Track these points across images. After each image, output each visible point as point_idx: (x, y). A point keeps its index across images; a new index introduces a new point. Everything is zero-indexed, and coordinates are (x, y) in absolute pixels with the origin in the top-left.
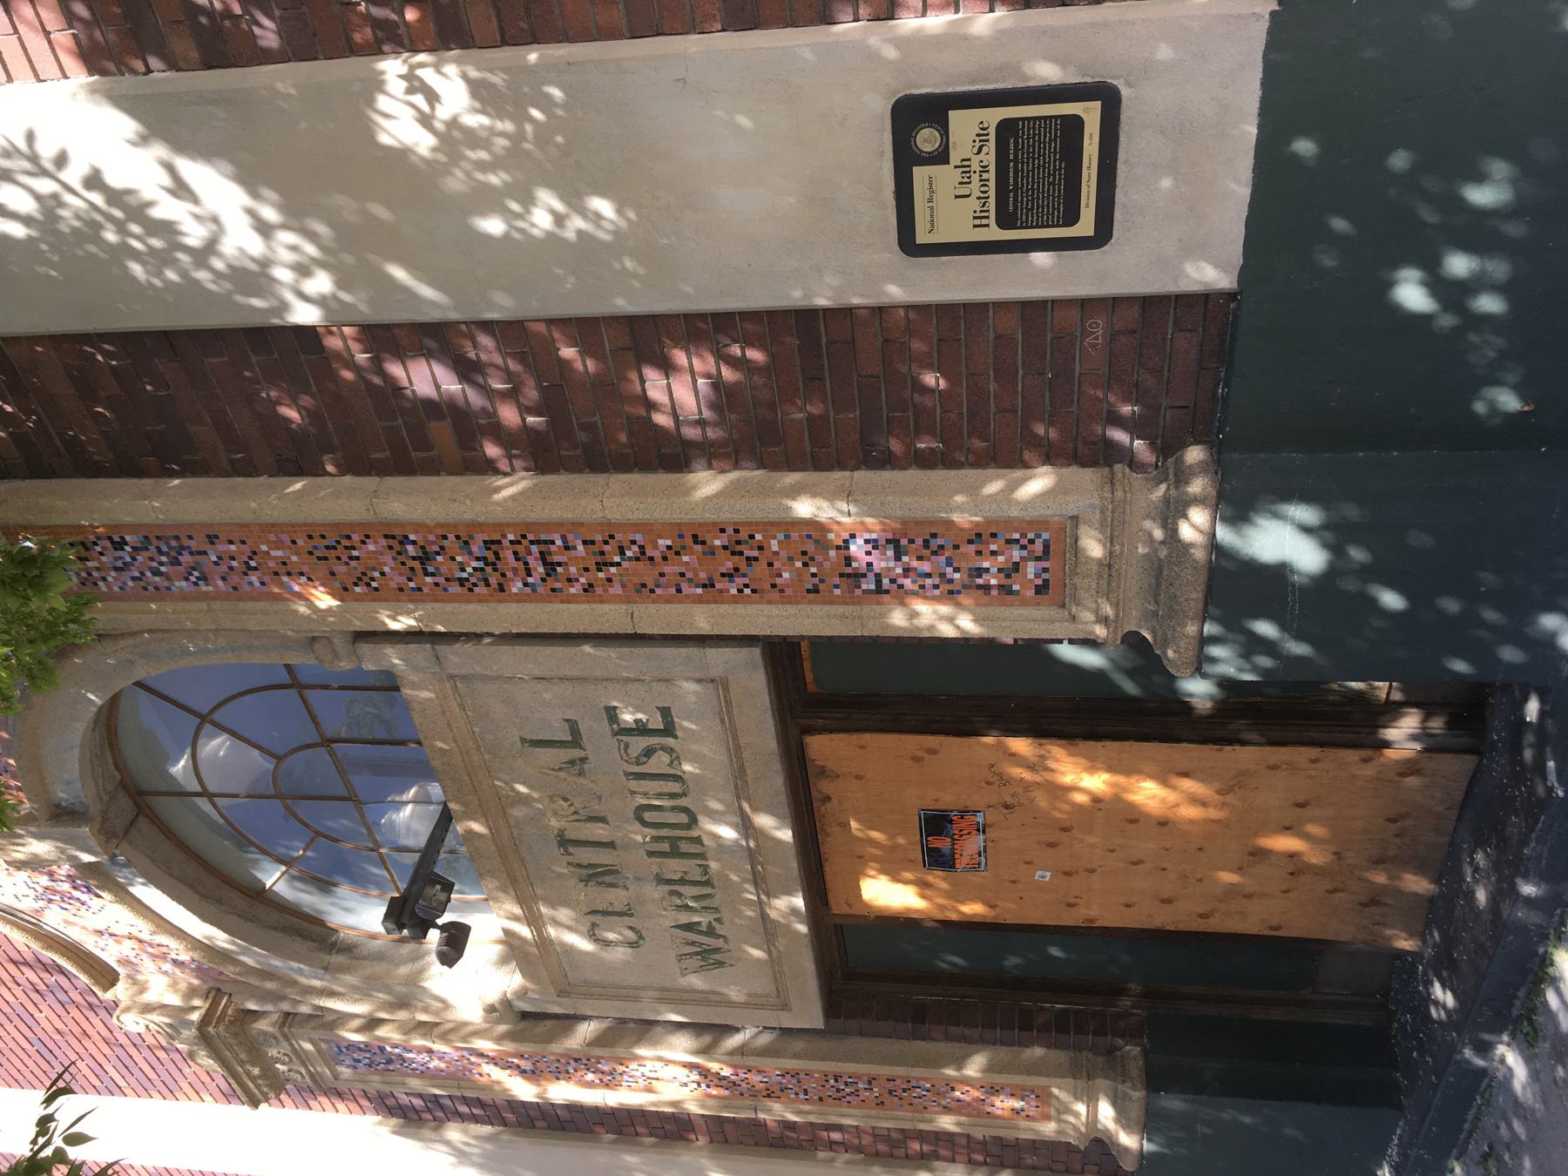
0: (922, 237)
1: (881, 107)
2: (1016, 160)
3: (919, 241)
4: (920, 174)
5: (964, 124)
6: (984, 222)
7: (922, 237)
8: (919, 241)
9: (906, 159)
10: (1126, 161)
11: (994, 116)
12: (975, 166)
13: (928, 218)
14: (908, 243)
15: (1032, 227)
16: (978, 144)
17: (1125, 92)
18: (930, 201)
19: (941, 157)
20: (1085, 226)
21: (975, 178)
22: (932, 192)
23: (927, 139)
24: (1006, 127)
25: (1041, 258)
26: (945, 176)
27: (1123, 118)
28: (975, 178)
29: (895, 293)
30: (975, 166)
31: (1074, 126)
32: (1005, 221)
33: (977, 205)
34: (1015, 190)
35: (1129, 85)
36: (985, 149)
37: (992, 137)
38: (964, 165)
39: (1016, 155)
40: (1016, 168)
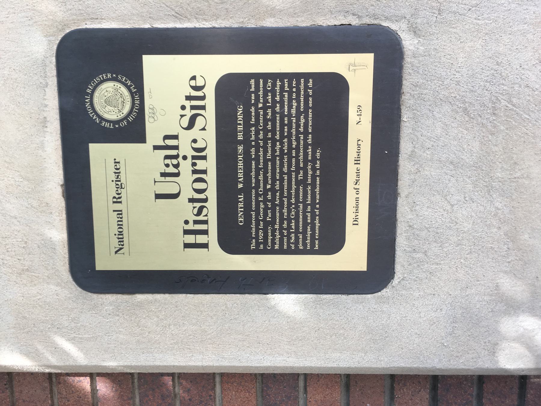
0: (105, 260)
1: (42, 49)
2: (246, 142)
3: (100, 265)
4: (101, 155)
5: (167, 77)
6: (201, 239)
7: (105, 260)
8: (100, 265)
9: (79, 131)
10: (412, 156)
11: (213, 67)
12: (186, 149)
13: (115, 229)
14: (87, 274)
15: (273, 252)
16: (189, 113)
17: (409, 43)
18: (117, 200)
19: (132, 130)
20: (353, 255)
21: (186, 167)
22: (119, 186)
23: (109, 100)
24: (232, 88)
25: (287, 303)
26: (138, 161)
27: (407, 85)
28: (186, 167)
29: (70, 352)
30: (186, 149)
31: (333, 89)
32: (233, 239)
33: (188, 211)
34: (247, 190)
35: (415, 31)
36: (200, 121)
37: (210, 102)
38: (168, 145)
39: (247, 133)
40: (247, 153)
